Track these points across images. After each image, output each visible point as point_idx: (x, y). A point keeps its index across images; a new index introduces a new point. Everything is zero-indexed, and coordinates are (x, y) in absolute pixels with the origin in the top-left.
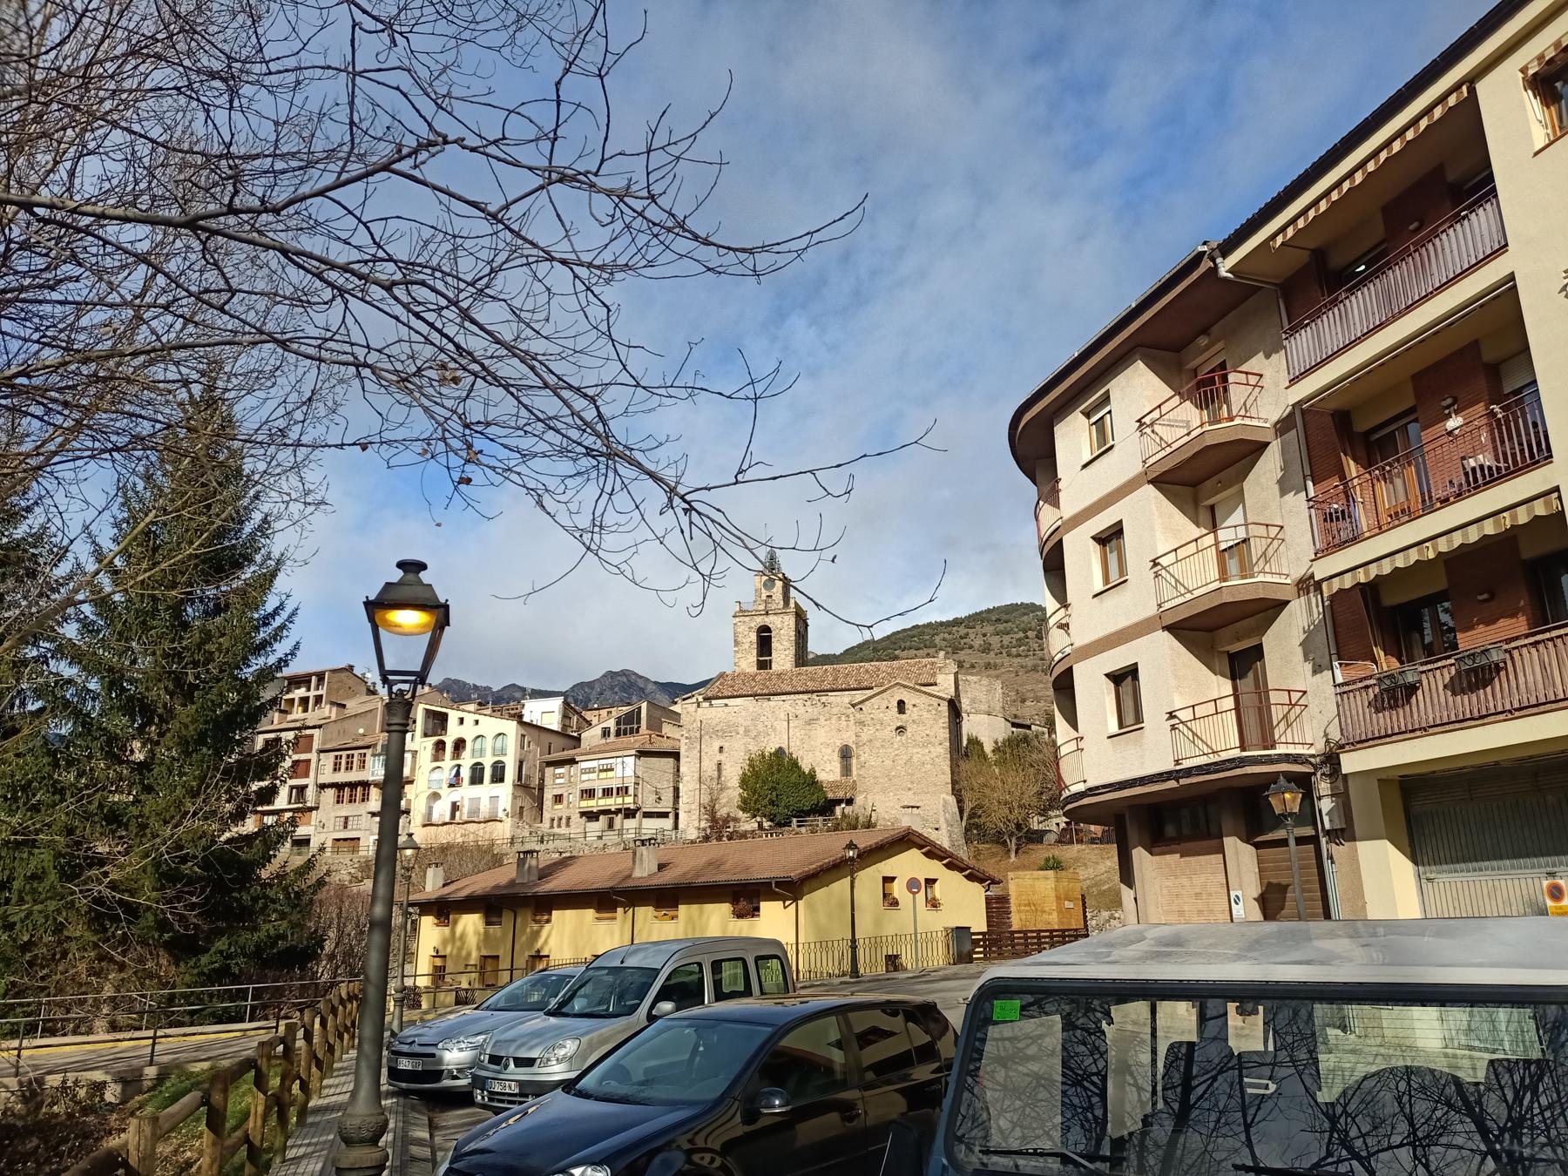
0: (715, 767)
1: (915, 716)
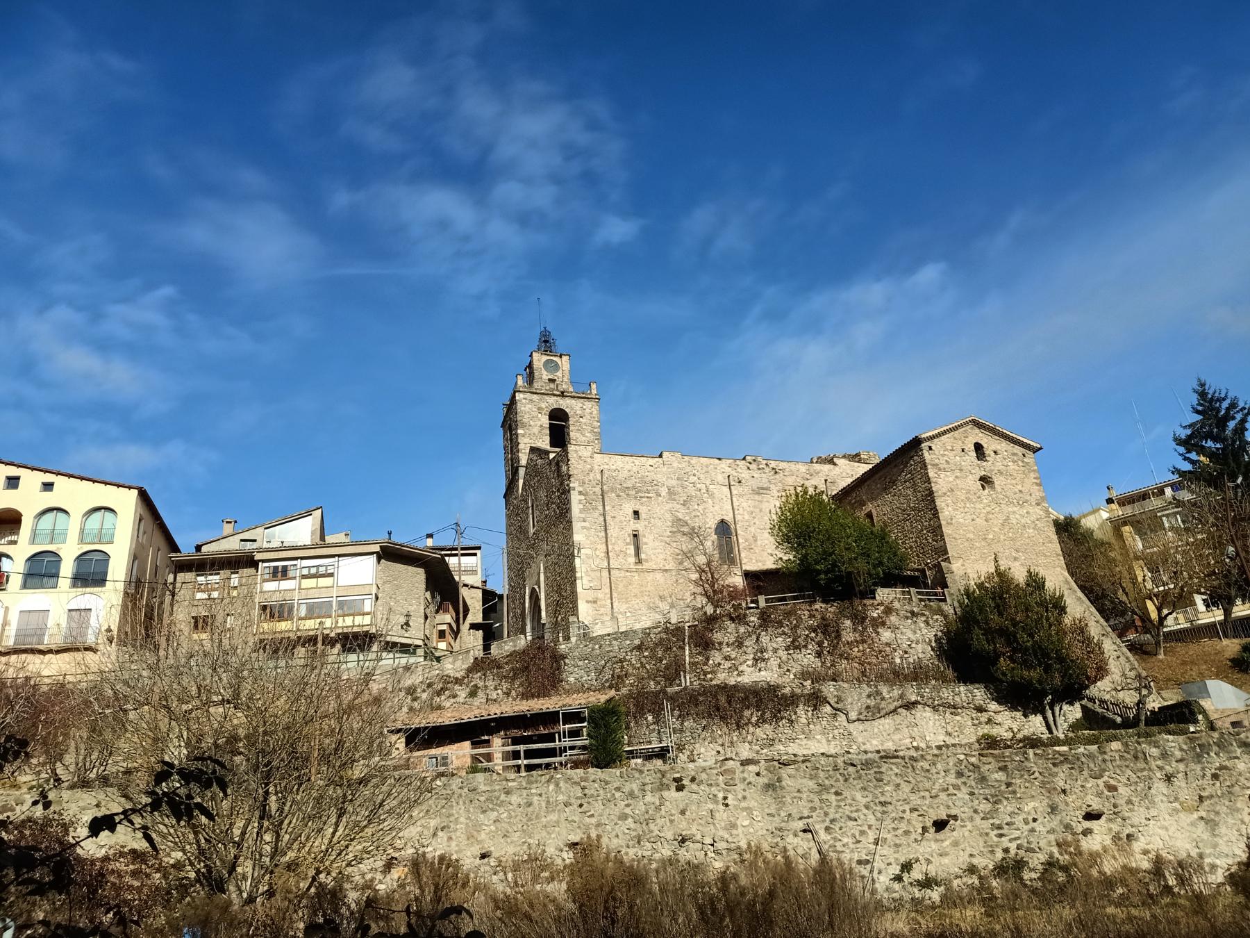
0: (629, 539)
1: (999, 466)
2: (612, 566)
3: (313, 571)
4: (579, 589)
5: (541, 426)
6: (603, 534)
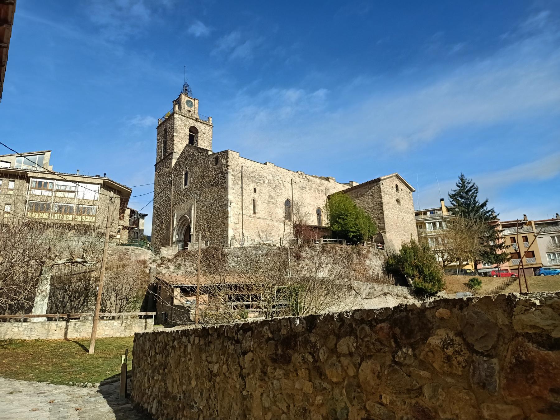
0: (252, 202)
2: (244, 214)
3: (63, 188)
4: (229, 223)
5: (185, 134)
6: (241, 197)
